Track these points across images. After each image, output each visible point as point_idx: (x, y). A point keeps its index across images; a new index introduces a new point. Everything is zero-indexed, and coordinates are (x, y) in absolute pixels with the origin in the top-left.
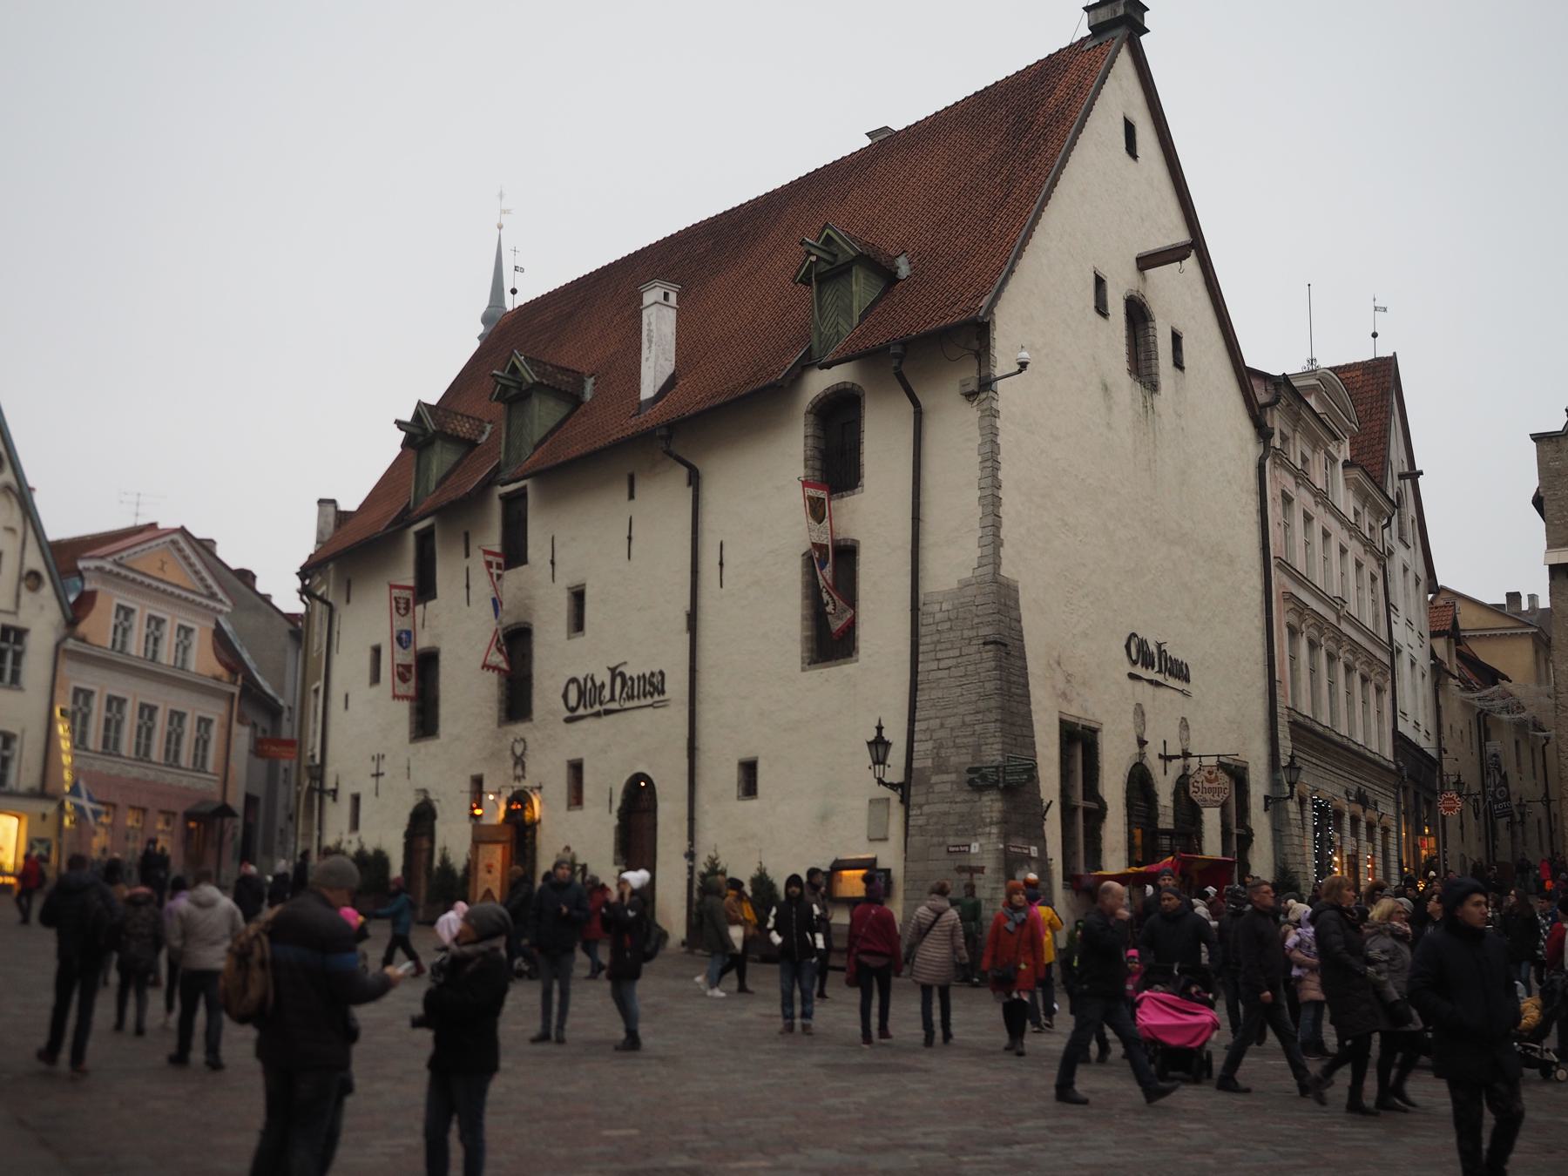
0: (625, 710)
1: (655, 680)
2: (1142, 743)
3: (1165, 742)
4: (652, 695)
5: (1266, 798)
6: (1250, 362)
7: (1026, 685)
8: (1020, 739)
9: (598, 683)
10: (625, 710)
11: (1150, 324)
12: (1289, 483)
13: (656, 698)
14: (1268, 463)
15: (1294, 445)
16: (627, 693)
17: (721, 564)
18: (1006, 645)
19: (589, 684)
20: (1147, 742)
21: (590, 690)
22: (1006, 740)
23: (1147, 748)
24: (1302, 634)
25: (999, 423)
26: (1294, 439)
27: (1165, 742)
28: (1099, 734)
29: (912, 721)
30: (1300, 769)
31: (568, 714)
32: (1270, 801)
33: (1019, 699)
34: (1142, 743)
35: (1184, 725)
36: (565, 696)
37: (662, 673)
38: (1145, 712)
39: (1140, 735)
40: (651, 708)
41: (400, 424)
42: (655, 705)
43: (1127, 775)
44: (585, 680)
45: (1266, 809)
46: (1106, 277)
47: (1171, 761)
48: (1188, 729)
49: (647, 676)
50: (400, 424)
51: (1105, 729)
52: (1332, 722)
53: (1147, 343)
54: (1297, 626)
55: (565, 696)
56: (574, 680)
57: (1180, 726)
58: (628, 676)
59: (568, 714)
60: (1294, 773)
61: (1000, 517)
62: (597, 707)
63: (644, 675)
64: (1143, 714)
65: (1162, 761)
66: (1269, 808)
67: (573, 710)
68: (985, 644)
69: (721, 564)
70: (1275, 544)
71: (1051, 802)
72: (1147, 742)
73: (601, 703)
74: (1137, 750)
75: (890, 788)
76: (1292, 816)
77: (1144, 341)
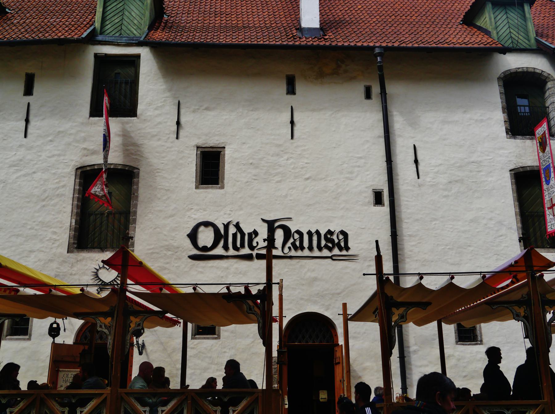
0: (291, 257)
1: (335, 237)
4: (330, 249)
9: (247, 230)
10: (291, 257)
13: (336, 251)
16: (294, 244)
17: (416, 161)
19: (232, 230)
21: (235, 235)
31: (195, 252)
36: (193, 236)
37: (344, 234)
40: (330, 260)
42: (334, 258)
44: (226, 227)
49: (323, 232)
55: (193, 236)
56: (207, 224)
58: (293, 231)
59: (195, 252)
62: (246, 251)
63: (318, 232)
67: (205, 249)
69: (416, 161)
73: (252, 248)
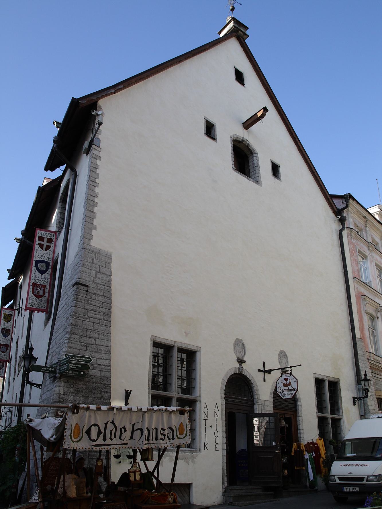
2: (241, 361)
3: (264, 363)
5: (354, 398)
6: (331, 191)
7: (109, 314)
8: (90, 347)
11: (254, 155)
12: (365, 249)
14: (345, 233)
15: (366, 233)
18: (87, 286)
20: (245, 362)
22: (72, 345)
23: (243, 365)
24: (378, 318)
25: (98, 162)
26: (366, 230)
27: (264, 363)
28: (198, 354)
29: (50, 343)
30: (369, 380)
32: (356, 400)
33: (96, 321)
34: (241, 361)
35: (283, 355)
38: (245, 344)
39: (241, 358)
41: (8, 270)
43: (226, 380)
45: (354, 404)
46: (216, 124)
47: (270, 373)
48: (287, 357)
50: (8, 270)
51: (203, 351)
52: (376, 350)
53: (253, 164)
54: (374, 314)
57: (279, 355)
60: (366, 383)
61: (93, 212)
64: (243, 344)
65: (262, 373)
66: (356, 403)
68: (73, 286)
70: (353, 272)
71: (131, 391)
72: (245, 362)
74: (237, 365)
75: (36, 387)
76: (370, 407)
77: (252, 163)
